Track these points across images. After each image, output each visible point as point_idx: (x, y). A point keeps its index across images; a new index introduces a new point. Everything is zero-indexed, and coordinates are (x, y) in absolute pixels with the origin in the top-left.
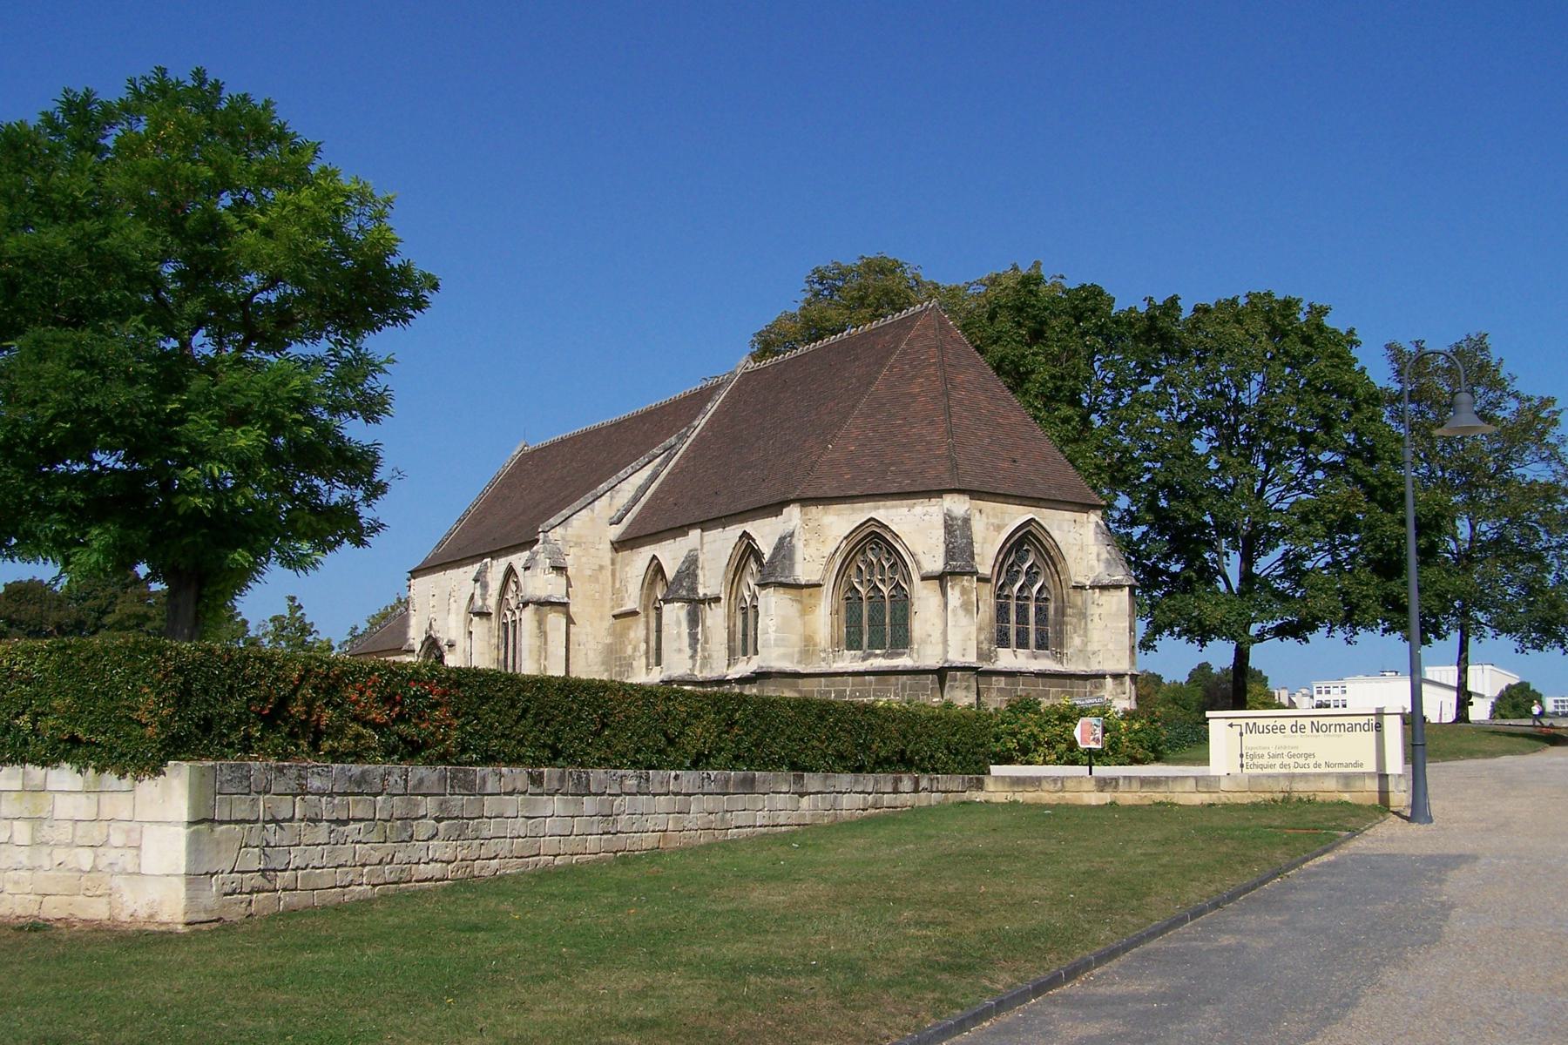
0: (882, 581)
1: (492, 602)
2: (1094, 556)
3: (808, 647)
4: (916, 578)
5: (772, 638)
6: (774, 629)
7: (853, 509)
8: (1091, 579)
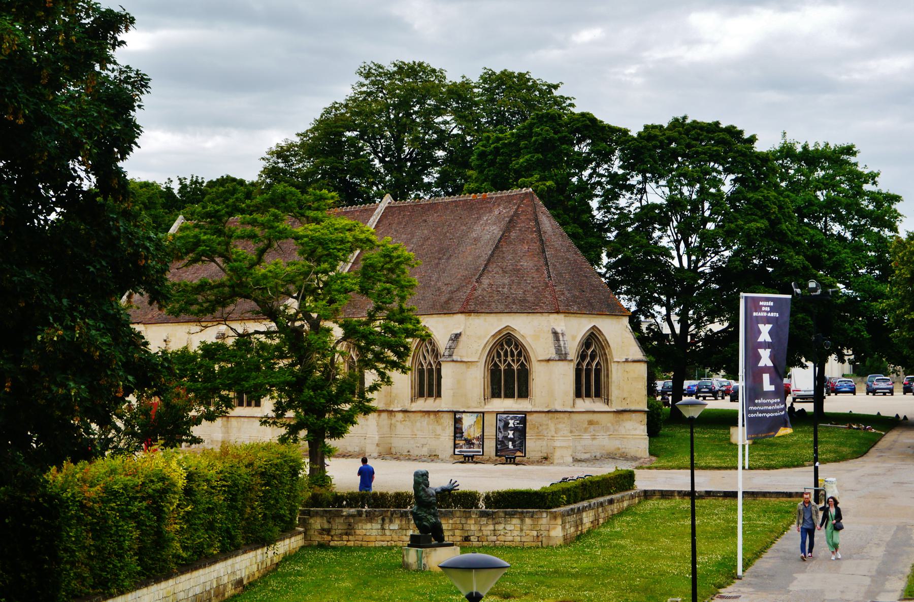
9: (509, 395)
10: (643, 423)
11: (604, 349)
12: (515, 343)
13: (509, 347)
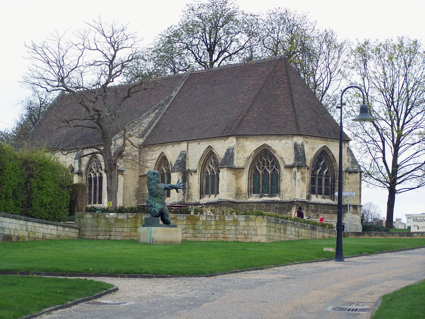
0: (268, 168)
1: (83, 169)
2: (347, 160)
3: (238, 193)
4: (282, 167)
5: (226, 188)
6: (226, 185)
7: (257, 140)
8: (345, 169)
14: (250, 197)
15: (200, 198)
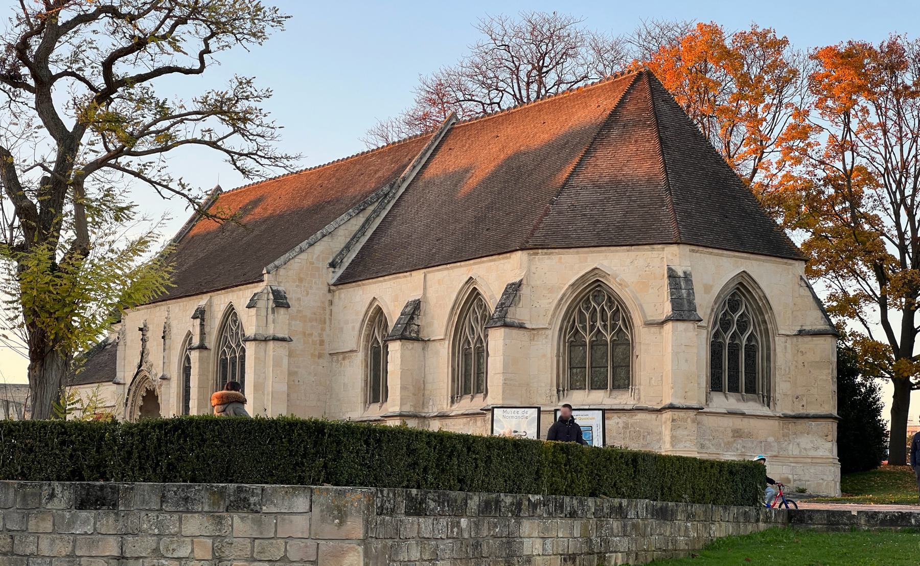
1: (211, 342)
4: (637, 320)
9: (598, 385)
10: (830, 438)
11: (762, 314)
12: (609, 298)
13: (599, 305)
14: (561, 398)
15: (453, 402)
